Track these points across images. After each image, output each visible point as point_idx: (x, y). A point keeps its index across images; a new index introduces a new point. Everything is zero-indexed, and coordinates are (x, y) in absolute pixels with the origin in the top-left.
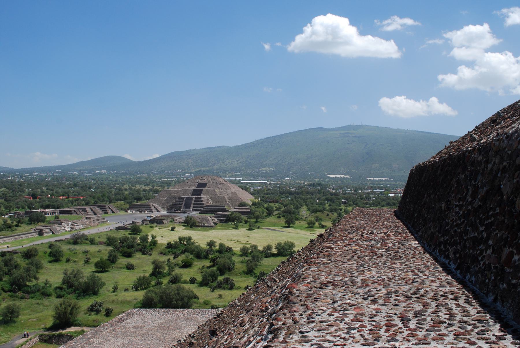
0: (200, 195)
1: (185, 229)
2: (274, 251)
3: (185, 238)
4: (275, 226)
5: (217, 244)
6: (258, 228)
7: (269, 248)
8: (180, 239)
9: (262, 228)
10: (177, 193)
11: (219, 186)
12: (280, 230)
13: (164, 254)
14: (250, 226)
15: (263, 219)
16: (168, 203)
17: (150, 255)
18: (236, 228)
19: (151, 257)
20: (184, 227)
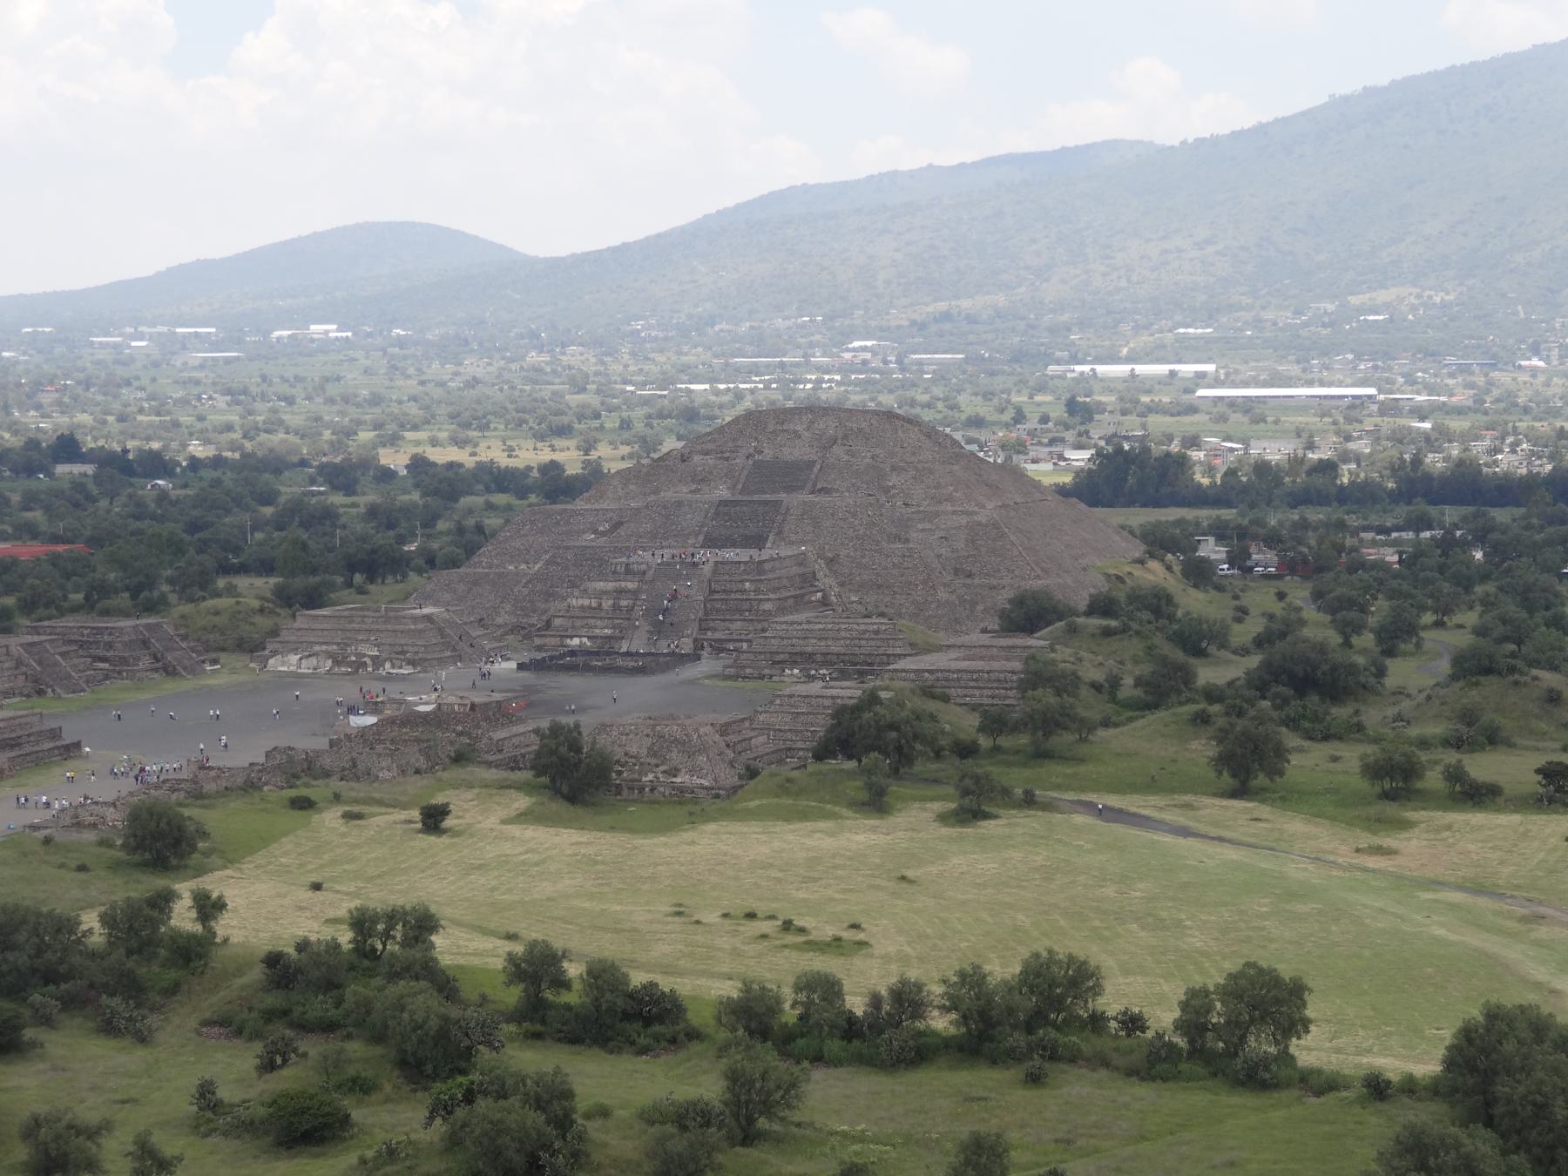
0: (758, 542)
1: (523, 817)
2: (941, 1023)
3: (392, 917)
4: (1151, 785)
5: (573, 970)
6: (1029, 801)
7: (907, 1000)
8: (362, 923)
9: (1048, 807)
10: (619, 524)
11: (894, 480)
12: (1167, 816)
13: (239, 1032)
14: (966, 793)
15: (1085, 728)
16: (549, 596)
17: (142, 1039)
18: (876, 803)
19: (141, 1053)
20: (522, 802)
